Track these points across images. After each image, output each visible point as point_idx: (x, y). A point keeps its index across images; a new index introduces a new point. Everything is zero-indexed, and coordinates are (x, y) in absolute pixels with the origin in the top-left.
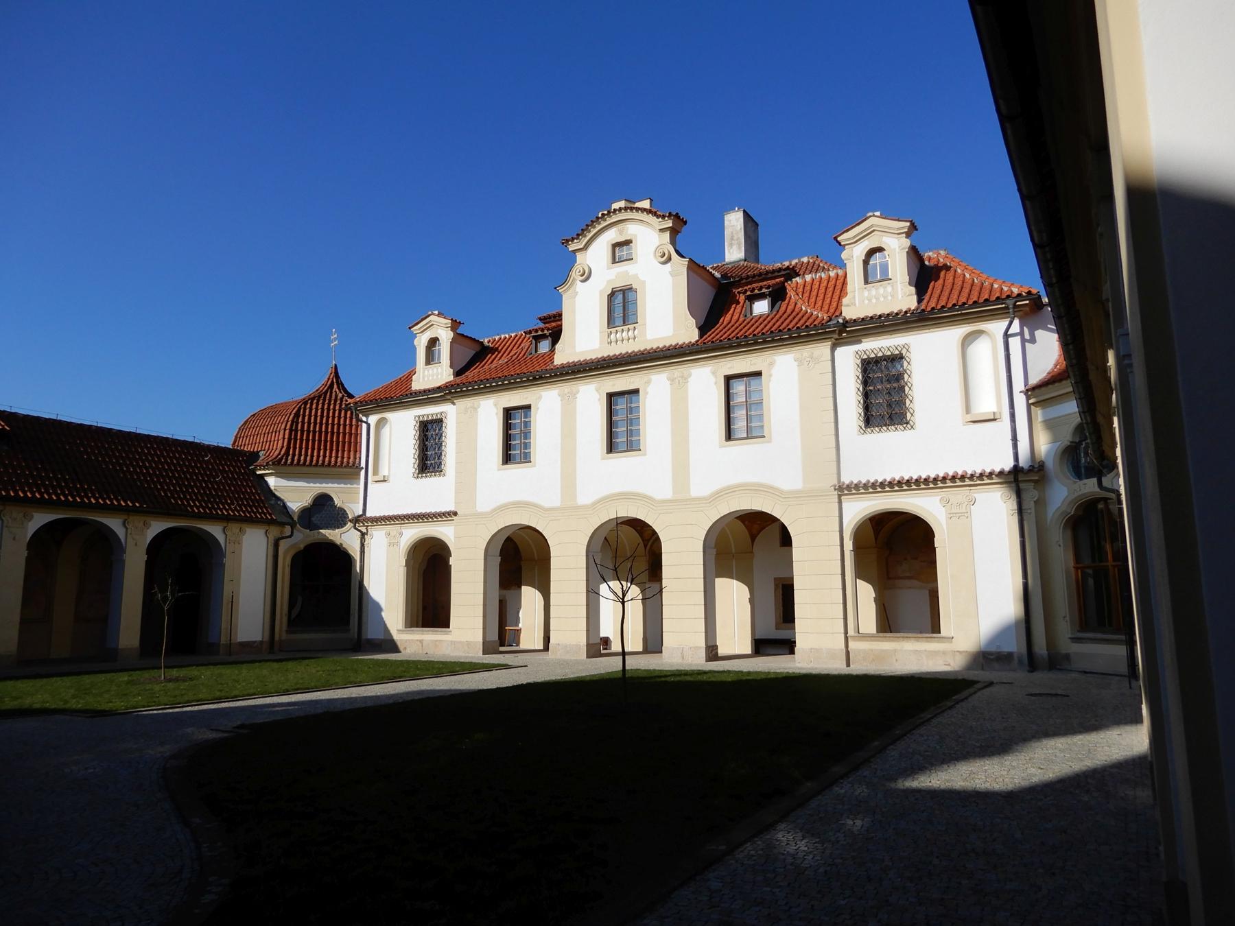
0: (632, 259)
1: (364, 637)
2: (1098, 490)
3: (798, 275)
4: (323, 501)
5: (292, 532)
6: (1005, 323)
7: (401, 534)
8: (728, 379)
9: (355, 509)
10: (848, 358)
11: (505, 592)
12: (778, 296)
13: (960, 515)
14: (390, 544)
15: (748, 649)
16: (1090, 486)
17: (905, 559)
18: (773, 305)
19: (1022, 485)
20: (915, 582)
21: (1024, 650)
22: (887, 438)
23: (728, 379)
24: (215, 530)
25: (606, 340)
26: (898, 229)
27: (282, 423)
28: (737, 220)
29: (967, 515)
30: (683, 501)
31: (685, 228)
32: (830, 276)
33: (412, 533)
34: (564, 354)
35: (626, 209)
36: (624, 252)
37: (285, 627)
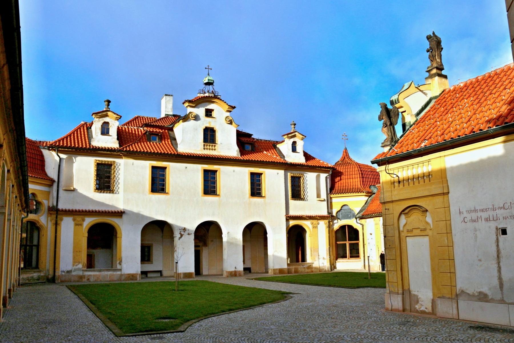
7: (84, 220)
13: (315, 227)
14: (76, 225)
33: (89, 221)
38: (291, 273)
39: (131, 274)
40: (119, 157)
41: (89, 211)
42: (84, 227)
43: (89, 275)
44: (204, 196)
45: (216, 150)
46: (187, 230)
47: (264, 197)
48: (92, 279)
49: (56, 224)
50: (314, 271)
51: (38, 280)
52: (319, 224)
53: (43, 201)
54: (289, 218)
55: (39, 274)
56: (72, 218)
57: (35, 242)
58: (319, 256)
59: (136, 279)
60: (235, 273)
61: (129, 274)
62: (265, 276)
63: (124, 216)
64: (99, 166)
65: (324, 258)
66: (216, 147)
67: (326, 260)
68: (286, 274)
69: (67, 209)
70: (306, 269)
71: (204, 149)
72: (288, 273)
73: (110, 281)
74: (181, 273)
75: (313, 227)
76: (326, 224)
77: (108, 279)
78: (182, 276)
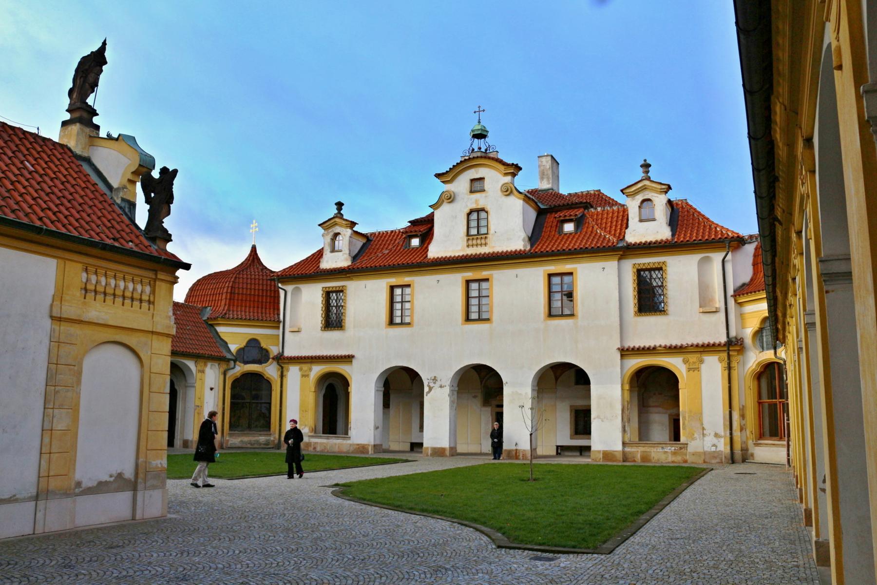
0: (484, 191)
2: (774, 357)
3: (592, 207)
4: (253, 343)
5: (235, 365)
6: (724, 254)
7: (311, 370)
8: (550, 276)
9: (274, 350)
10: (629, 266)
12: (579, 222)
13: (694, 369)
14: (303, 376)
15: (554, 453)
16: (768, 355)
17: (655, 394)
18: (577, 227)
19: (731, 353)
20: (660, 409)
23: (550, 276)
24: (191, 364)
25: (465, 244)
26: (661, 189)
27: (224, 288)
28: (547, 162)
31: (520, 173)
32: (613, 210)
33: (318, 370)
34: (435, 251)
35: (481, 157)
36: (477, 185)
38: (519, 459)
39: (361, 444)
40: (349, 278)
42: (311, 379)
43: (316, 443)
44: (465, 324)
45: (488, 246)
46: (439, 380)
47: (409, 324)
48: (318, 449)
49: (282, 376)
50: (689, 461)
51: (264, 444)
52: (702, 362)
53: (271, 347)
54: (626, 352)
55: (267, 438)
56: (718, 357)
58: (703, 429)
59: (368, 452)
60: (516, 453)
61: (358, 445)
62: (559, 462)
63: (354, 361)
64: (328, 294)
65: (716, 435)
66: (488, 241)
67: (722, 440)
68: (620, 461)
69: (706, 342)
70: (670, 455)
71: (468, 246)
72: (624, 461)
73: (339, 452)
74: (427, 448)
75: (689, 370)
76: (721, 361)
77: (336, 449)
78: (430, 452)
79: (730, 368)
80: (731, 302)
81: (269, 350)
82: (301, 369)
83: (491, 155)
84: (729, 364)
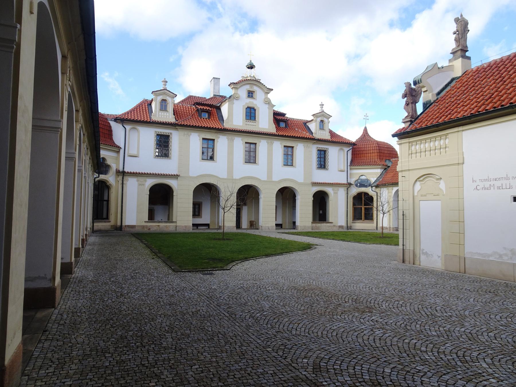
1: (123, 224)
7: (146, 181)
11: (153, 206)
13: (336, 193)
14: (140, 185)
21: (346, 225)
22: (322, 172)
29: (337, 193)
30: (270, 182)
33: (150, 182)
37: (352, 219)
41: (131, 173)
52: (338, 190)
57: (106, 198)
79: (347, 193)
80: (349, 167)
81: (111, 166)
82: (138, 181)
83: (258, 81)
84: (347, 192)
